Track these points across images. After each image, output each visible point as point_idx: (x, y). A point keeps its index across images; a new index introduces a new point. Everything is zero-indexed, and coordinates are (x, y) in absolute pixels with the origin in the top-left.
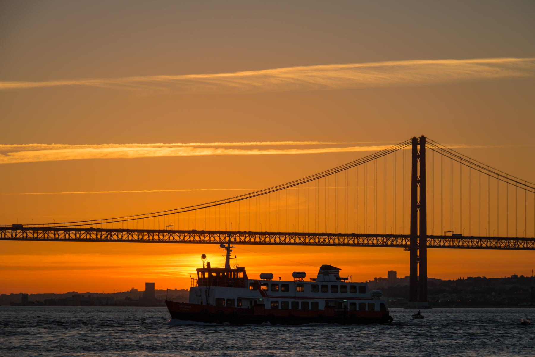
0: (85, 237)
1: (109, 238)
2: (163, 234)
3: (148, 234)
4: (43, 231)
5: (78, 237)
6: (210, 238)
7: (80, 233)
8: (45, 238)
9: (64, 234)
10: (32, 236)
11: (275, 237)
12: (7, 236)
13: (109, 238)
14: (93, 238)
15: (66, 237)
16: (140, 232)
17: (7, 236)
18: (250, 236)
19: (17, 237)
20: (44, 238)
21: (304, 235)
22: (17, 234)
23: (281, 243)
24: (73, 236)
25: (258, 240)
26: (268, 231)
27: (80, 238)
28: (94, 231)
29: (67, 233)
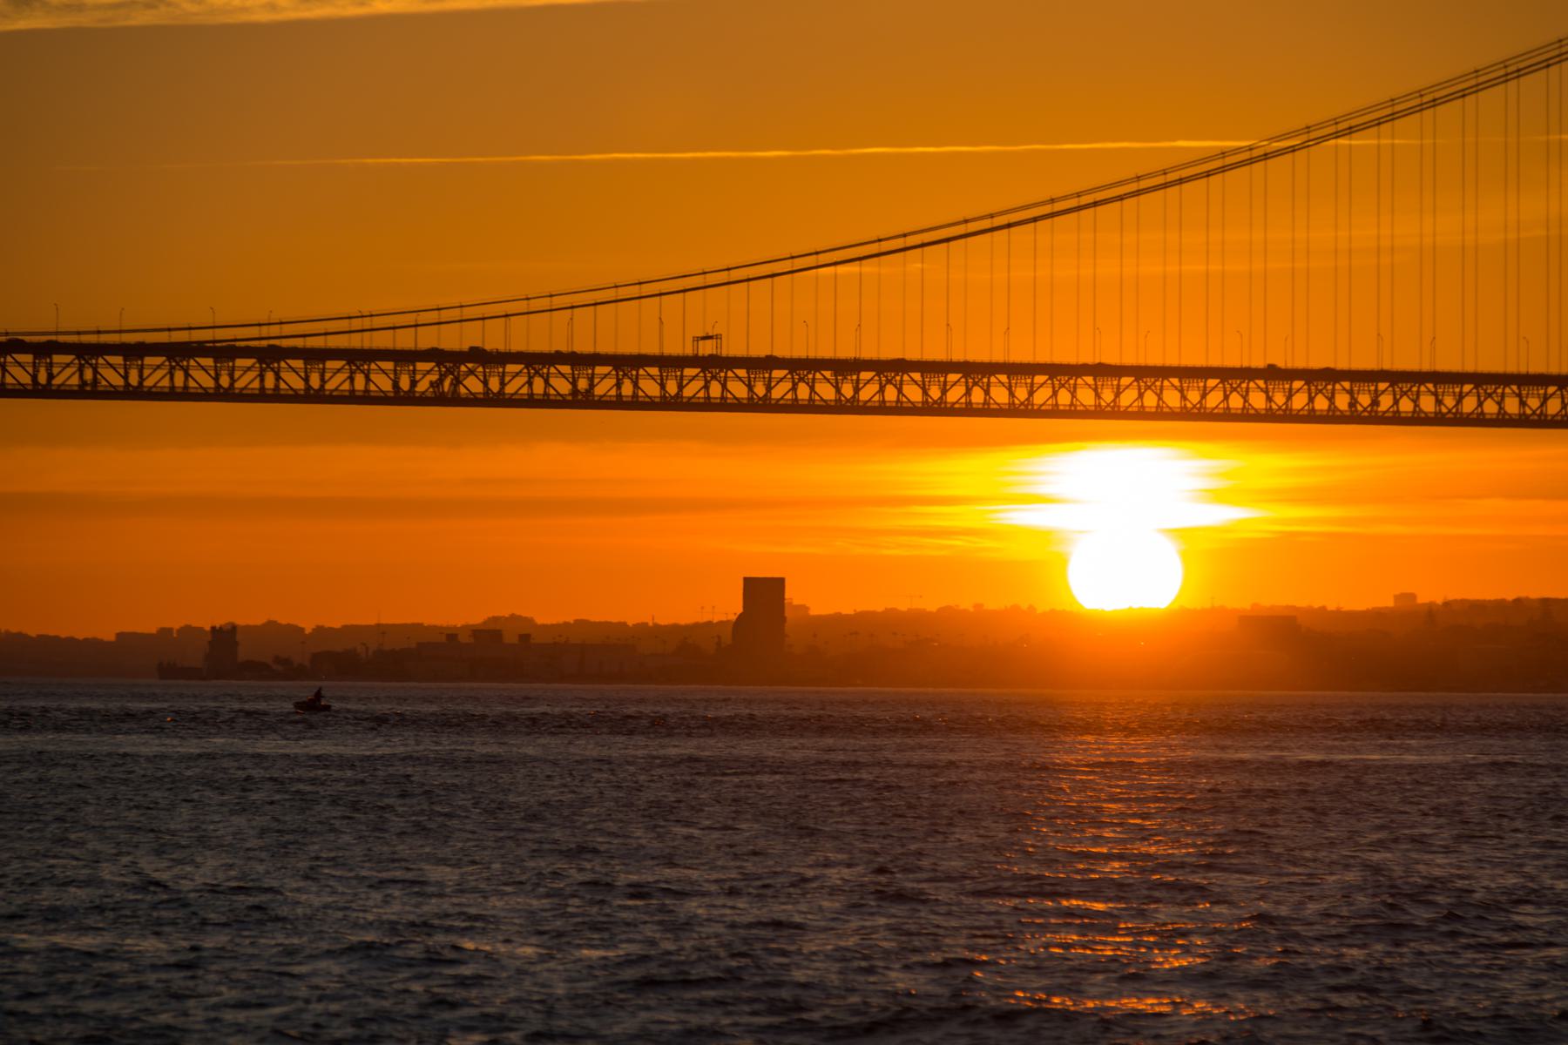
0: (525, 390)
1: (446, 389)
2: (679, 373)
3: (614, 372)
4: (438, 365)
5: (761, 394)
6: (1226, 397)
7: (504, 372)
8: (532, 394)
9: (526, 379)
10: (481, 385)
11: (1418, 392)
12: (376, 389)
13: (446, 389)
14: (559, 394)
15: (623, 394)
16: (1359, 381)
17: (523, 386)
18: (1394, 391)
19: (417, 389)
20: (532, 394)
21: (1457, 384)
22: (418, 377)
23: (1528, 417)
24: (739, 390)
25: (1428, 404)
26: (1387, 366)
27: (504, 394)
28: (563, 364)
29: (537, 372)
